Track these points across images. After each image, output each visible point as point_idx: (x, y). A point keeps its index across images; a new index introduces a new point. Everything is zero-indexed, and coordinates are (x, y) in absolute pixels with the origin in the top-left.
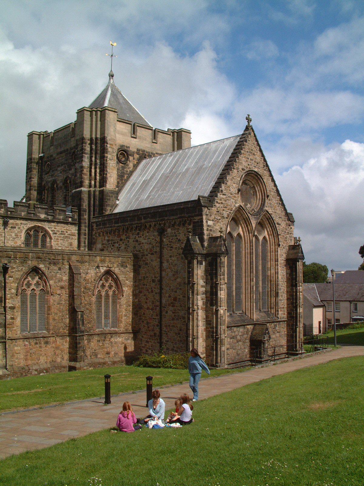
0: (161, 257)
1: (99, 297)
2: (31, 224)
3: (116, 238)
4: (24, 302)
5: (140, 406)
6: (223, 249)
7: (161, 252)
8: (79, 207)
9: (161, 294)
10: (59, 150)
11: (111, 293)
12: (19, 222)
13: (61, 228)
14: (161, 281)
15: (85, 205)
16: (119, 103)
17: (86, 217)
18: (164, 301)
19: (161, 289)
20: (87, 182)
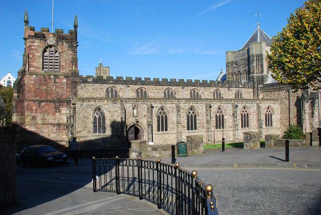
0: (289, 100)
1: (266, 115)
2: (237, 89)
3: (269, 93)
4: (242, 118)
5: (277, 158)
6: (317, 97)
7: (289, 98)
8: (253, 81)
9: (289, 114)
10: (241, 58)
11: (270, 114)
12: (233, 89)
13: (247, 90)
14: (289, 109)
15: (255, 81)
16: (263, 37)
17: (256, 85)
18: (291, 116)
19: (289, 112)
20: (255, 72)
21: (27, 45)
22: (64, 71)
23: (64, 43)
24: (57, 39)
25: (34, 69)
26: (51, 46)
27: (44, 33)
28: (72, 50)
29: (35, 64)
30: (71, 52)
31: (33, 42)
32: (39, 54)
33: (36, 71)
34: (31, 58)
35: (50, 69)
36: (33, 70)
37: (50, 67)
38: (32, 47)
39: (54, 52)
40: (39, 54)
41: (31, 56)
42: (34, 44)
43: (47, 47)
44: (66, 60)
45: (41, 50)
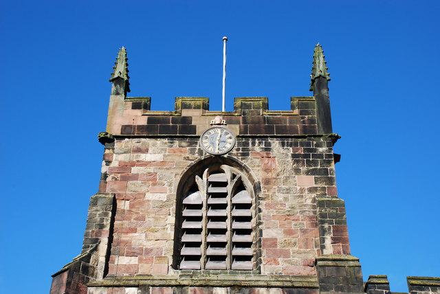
21: (115, 164)
22: (281, 266)
23: (275, 144)
24: (245, 130)
25: (134, 261)
26: (214, 163)
27: (185, 113)
28: (307, 173)
29: (138, 239)
30: (309, 181)
31: (139, 150)
32: (164, 197)
33: (144, 269)
34: (126, 215)
35: (210, 264)
36: (128, 267)
37: (212, 251)
38: (135, 170)
39: (229, 189)
40: (167, 193)
41: (123, 205)
42: (144, 157)
43: (197, 168)
44: (288, 216)
45: (173, 180)
